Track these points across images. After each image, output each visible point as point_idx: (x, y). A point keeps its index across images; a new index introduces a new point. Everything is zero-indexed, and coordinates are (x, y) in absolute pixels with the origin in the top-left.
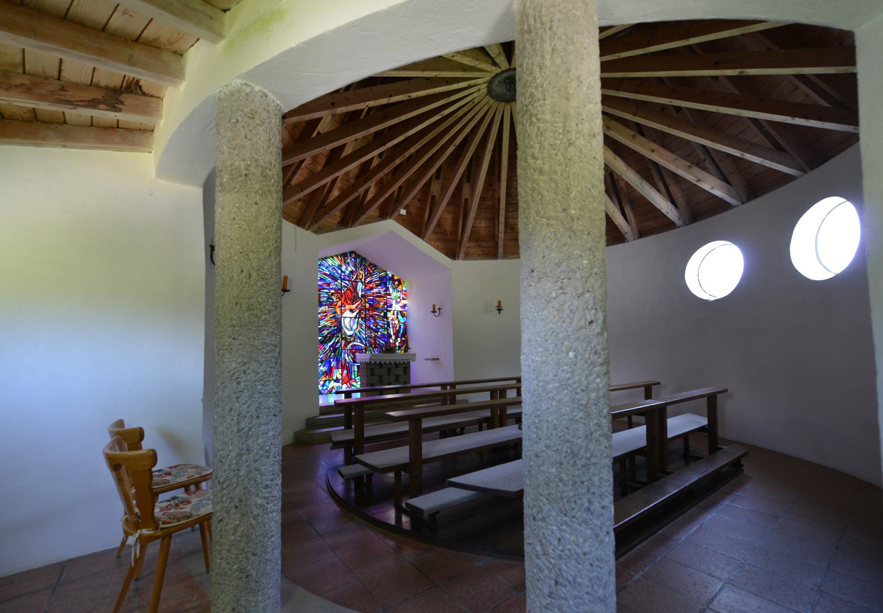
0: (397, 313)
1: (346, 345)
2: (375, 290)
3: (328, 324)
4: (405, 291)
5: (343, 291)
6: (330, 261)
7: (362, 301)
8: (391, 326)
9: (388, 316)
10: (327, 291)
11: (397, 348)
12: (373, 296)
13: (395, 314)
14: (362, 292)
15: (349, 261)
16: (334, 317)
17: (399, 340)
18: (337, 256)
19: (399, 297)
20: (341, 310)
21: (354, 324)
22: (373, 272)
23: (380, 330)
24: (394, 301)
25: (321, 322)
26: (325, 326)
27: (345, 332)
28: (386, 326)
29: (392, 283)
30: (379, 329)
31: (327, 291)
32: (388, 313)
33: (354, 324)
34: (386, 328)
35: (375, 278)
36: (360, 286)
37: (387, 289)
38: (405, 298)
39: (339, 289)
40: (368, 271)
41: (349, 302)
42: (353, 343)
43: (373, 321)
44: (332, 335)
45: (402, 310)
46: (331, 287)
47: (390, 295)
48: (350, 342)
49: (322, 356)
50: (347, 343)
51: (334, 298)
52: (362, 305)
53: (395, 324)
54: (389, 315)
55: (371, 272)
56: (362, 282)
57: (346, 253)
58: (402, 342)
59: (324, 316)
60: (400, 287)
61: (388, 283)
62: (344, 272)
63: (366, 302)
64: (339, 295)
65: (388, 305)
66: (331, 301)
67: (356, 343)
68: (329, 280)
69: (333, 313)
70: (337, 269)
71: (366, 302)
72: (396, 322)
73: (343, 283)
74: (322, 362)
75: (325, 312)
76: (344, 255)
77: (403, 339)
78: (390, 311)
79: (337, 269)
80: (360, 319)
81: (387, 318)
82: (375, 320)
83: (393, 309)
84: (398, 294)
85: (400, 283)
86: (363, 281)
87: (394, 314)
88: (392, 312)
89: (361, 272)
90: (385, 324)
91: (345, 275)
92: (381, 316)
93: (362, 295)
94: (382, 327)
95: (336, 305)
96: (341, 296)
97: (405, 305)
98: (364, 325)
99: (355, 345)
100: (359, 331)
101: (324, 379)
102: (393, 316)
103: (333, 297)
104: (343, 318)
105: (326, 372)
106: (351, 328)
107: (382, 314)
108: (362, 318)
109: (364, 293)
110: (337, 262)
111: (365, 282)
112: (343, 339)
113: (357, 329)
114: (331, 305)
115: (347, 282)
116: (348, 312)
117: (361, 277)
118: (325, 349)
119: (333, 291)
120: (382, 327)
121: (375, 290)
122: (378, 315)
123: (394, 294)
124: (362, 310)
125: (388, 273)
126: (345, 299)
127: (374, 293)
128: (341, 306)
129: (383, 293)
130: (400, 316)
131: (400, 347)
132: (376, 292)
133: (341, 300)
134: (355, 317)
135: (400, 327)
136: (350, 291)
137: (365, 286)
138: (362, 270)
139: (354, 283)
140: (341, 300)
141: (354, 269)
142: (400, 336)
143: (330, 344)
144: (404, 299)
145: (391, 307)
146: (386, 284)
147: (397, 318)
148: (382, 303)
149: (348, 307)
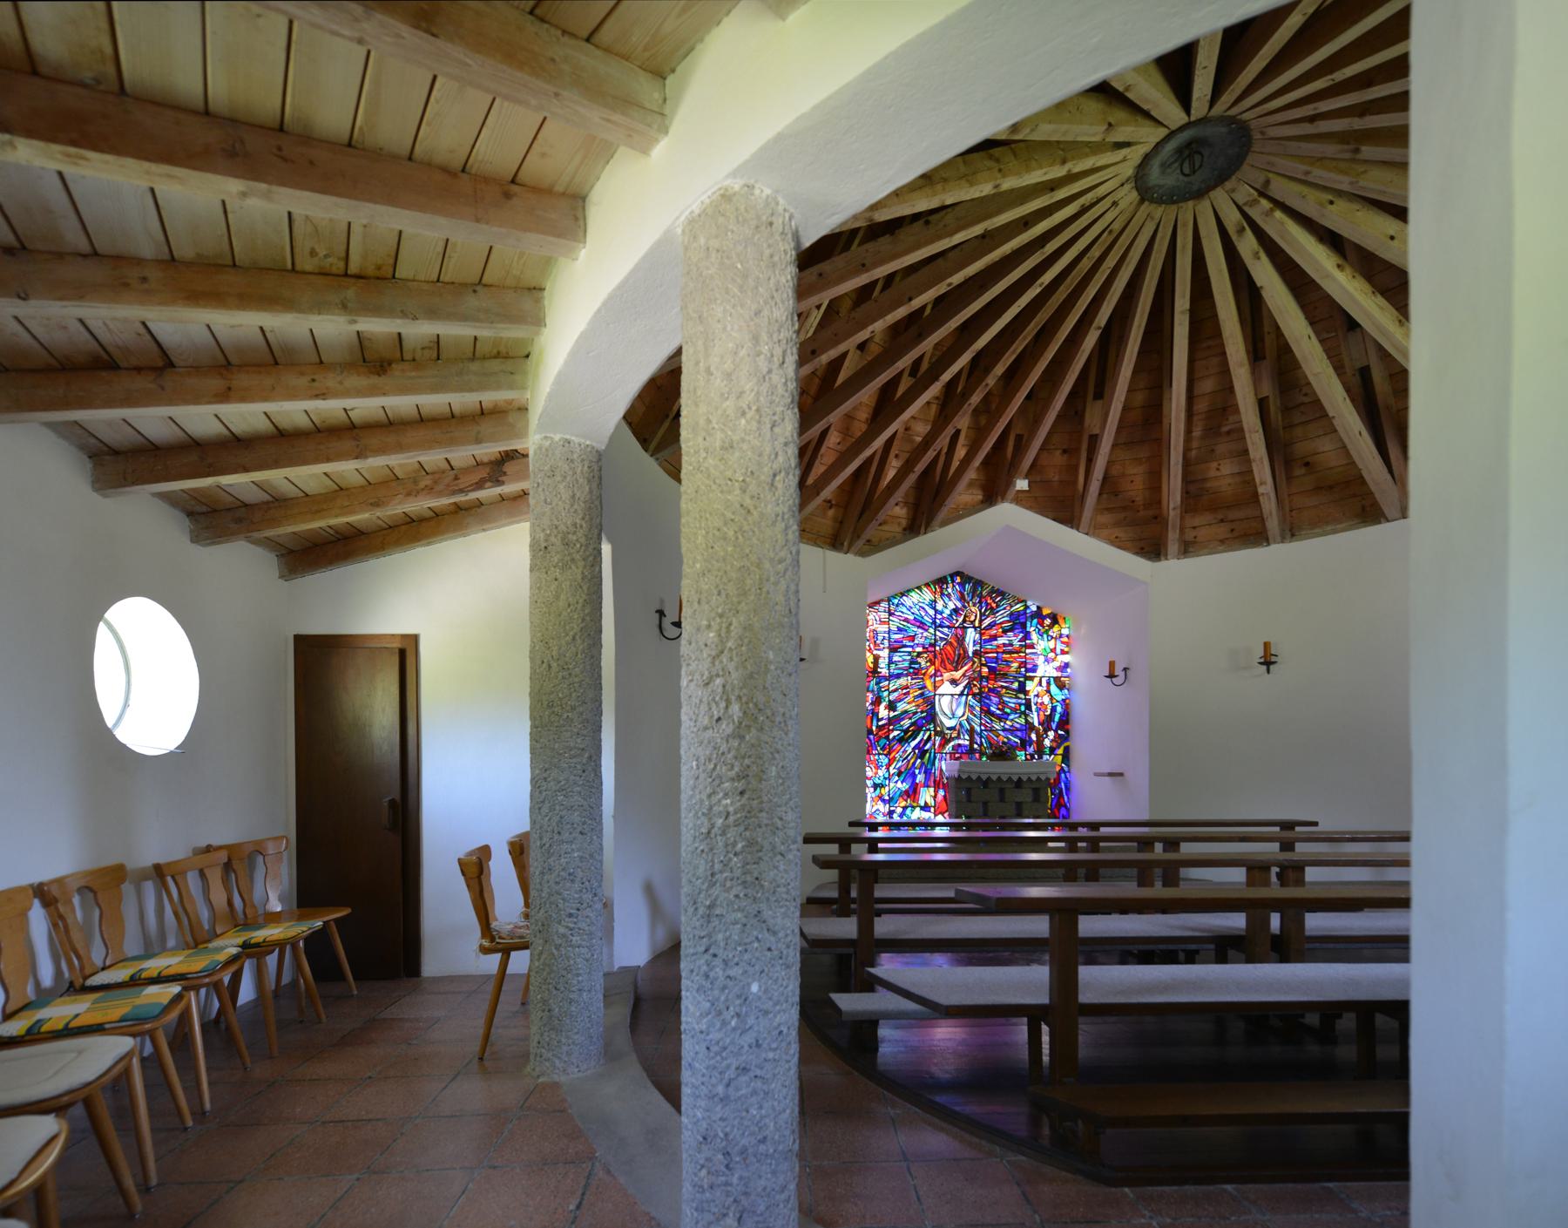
0: (1048, 683)
1: (943, 745)
2: (1001, 641)
3: (911, 708)
4: (1067, 636)
5: (937, 648)
6: (914, 596)
7: (974, 663)
8: (1034, 707)
9: (1027, 688)
10: (910, 649)
11: (1047, 751)
12: (997, 653)
13: (1044, 683)
14: (974, 645)
15: (950, 590)
16: (922, 694)
17: (1051, 734)
18: (927, 585)
19: (1053, 650)
20: (935, 682)
21: (958, 706)
22: (998, 606)
23: (1011, 717)
24: (1042, 659)
25: (898, 704)
26: (906, 712)
27: (941, 722)
28: (1023, 708)
29: (1038, 623)
30: (1009, 715)
31: (910, 649)
32: (1028, 683)
33: (958, 706)
34: (1024, 713)
35: (1002, 616)
36: (971, 635)
37: (1027, 636)
38: (1066, 649)
39: (931, 645)
40: (987, 604)
41: (949, 666)
42: (956, 742)
43: (995, 700)
44: (917, 727)
45: (1059, 674)
46: (916, 642)
47: (1032, 646)
48: (952, 739)
49: (900, 764)
50: (945, 742)
51: (922, 661)
52: (974, 671)
53: (1042, 704)
54: (1030, 686)
55: (994, 605)
56: (974, 627)
57: (945, 578)
58: (1060, 740)
59: (905, 694)
60: (1056, 628)
61: (1028, 624)
62: (941, 613)
63: (982, 665)
64: (931, 655)
65: (1029, 666)
66: (916, 666)
67: (961, 742)
68: (913, 629)
69: (920, 689)
70: (927, 608)
71: (982, 665)
72: (1046, 699)
73: (938, 633)
74: (899, 774)
75: (907, 687)
76: (941, 581)
77: (1060, 732)
78: (1031, 679)
79: (927, 608)
80: (970, 697)
81: (1026, 693)
82: (1000, 696)
83: (1039, 673)
84: (1052, 644)
85: (1055, 620)
86: (977, 624)
87: (1040, 684)
88: (1037, 680)
89: (973, 609)
90: (1020, 705)
91: (943, 618)
92: (1013, 690)
93: (975, 653)
94: (1014, 710)
95: (924, 674)
96: (935, 657)
97: (1066, 665)
98: (978, 709)
99: (959, 745)
100: (968, 720)
101: (903, 804)
102: (1039, 689)
103: (919, 660)
104: (937, 697)
105: (906, 792)
106: (953, 714)
107: (1016, 685)
108: (974, 695)
109: (978, 647)
110: (927, 595)
111: (980, 627)
112: (937, 733)
113: (963, 715)
114: (916, 674)
115: (945, 630)
116: (947, 684)
117: (973, 618)
118: (905, 751)
119: (919, 649)
120: (1014, 710)
121: (1001, 641)
122: (1006, 688)
123: (1042, 644)
124: (974, 679)
125: (1029, 603)
126: (942, 661)
127: (998, 646)
128: (935, 675)
129: (1016, 643)
130: (1054, 689)
131: (1052, 751)
132: (1004, 645)
133: (934, 664)
134: (962, 694)
135: (1054, 709)
136: (951, 644)
137: (981, 634)
138: (974, 605)
139: (959, 631)
140: (934, 664)
141: (959, 605)
142: (1054, 726)
143: (913, 744)
144: (1063, 652)
145: (1034, 669)
146: (1024, 626)
147: (1048, 691)
148: (1015, 665)
149: (947, 675)
